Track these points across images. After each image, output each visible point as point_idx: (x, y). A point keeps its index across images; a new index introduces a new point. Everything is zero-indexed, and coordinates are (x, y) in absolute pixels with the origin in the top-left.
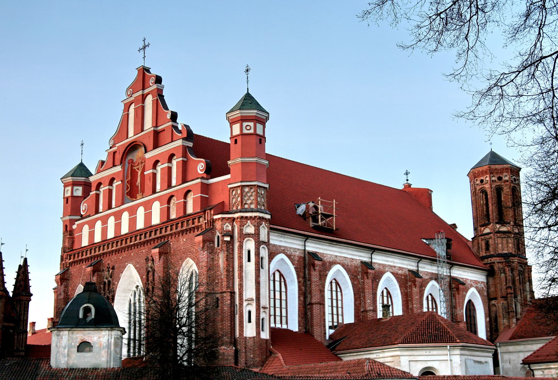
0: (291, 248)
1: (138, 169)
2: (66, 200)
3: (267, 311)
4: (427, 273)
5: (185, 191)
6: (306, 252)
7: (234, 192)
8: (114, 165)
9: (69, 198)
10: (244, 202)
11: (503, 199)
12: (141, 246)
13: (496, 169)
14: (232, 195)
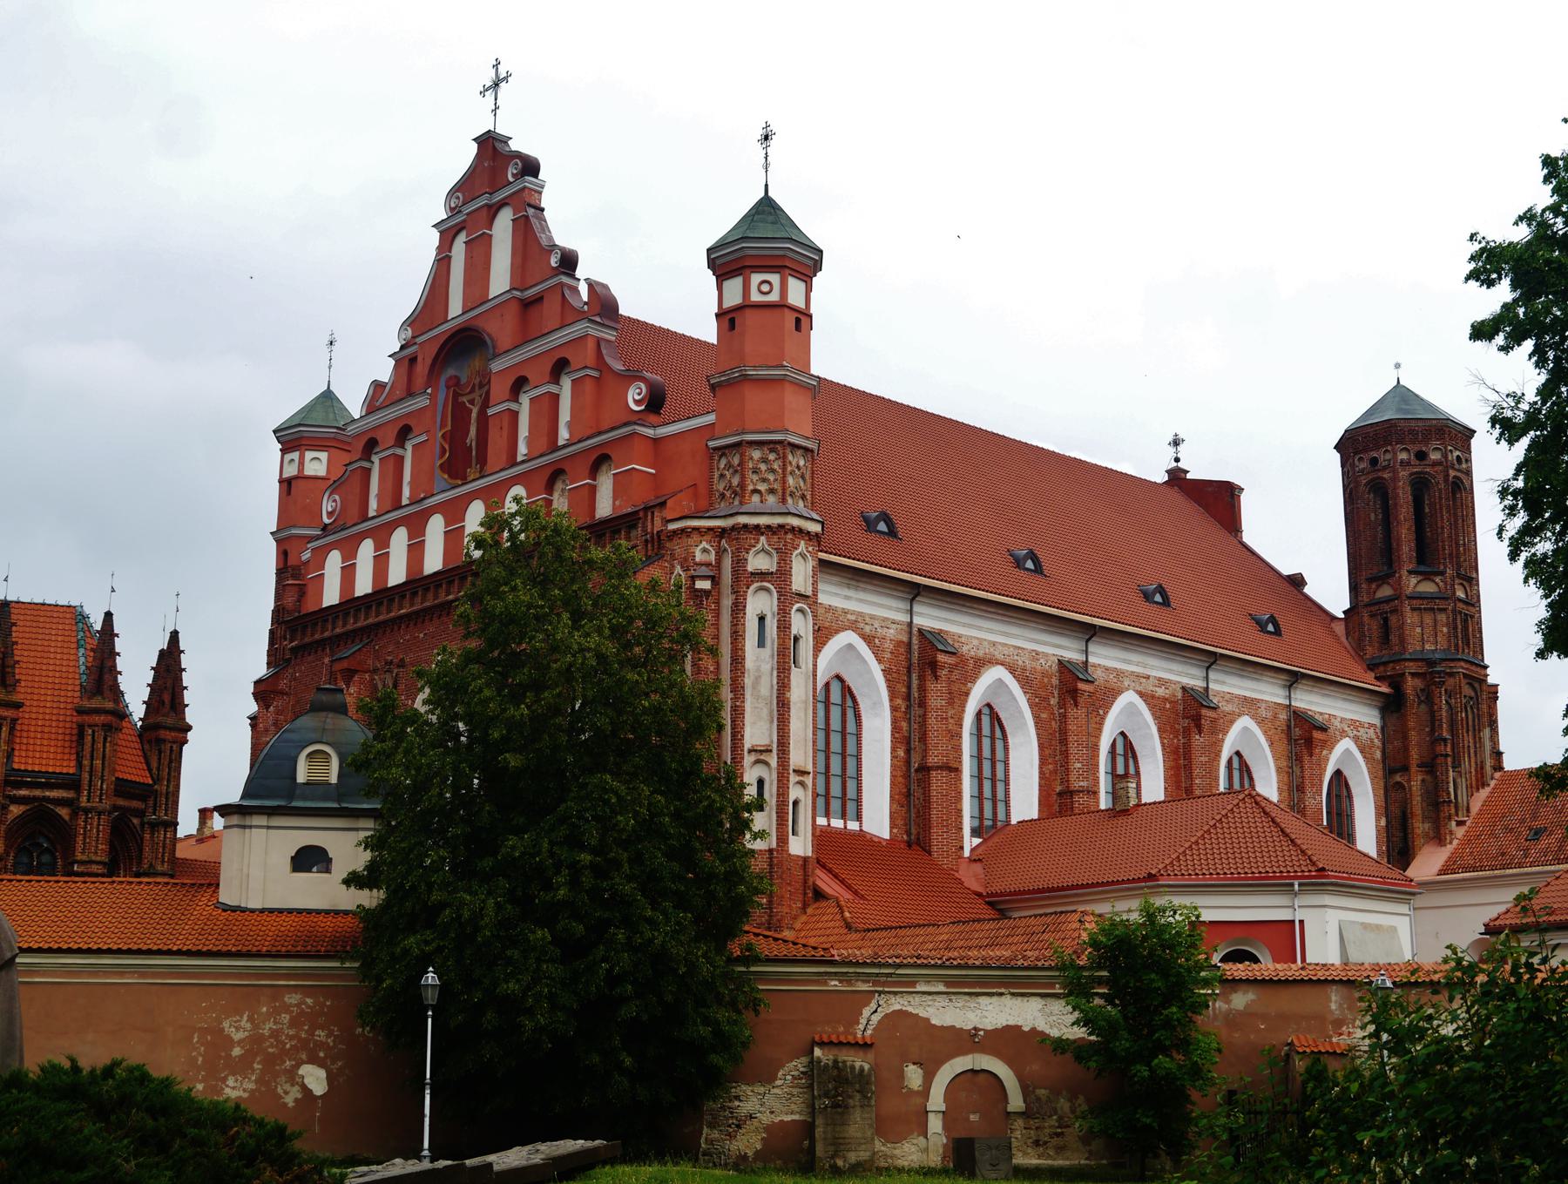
0: (873, 617)
1: (472, 402)
2: (287, 484)
3: (809, 780)
4: (1232, 698)
5: (595, 456)
6: (915, 630)
7: (723, 462)
8: (410, 394)
9: (293, 483)
10: (751, 487)
11: (1427, 510)
13: (1411, 431)
14: (718, 469)
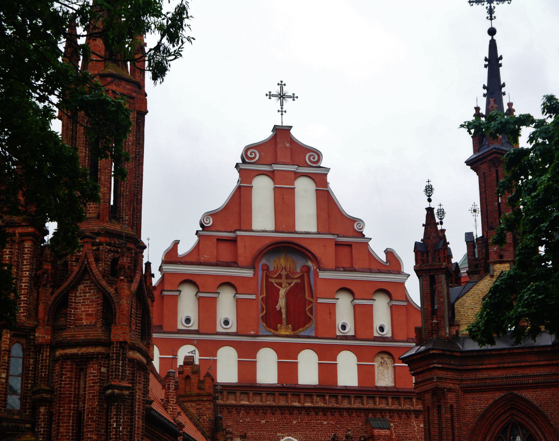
1: (280, 284)
12: (316, 414)
